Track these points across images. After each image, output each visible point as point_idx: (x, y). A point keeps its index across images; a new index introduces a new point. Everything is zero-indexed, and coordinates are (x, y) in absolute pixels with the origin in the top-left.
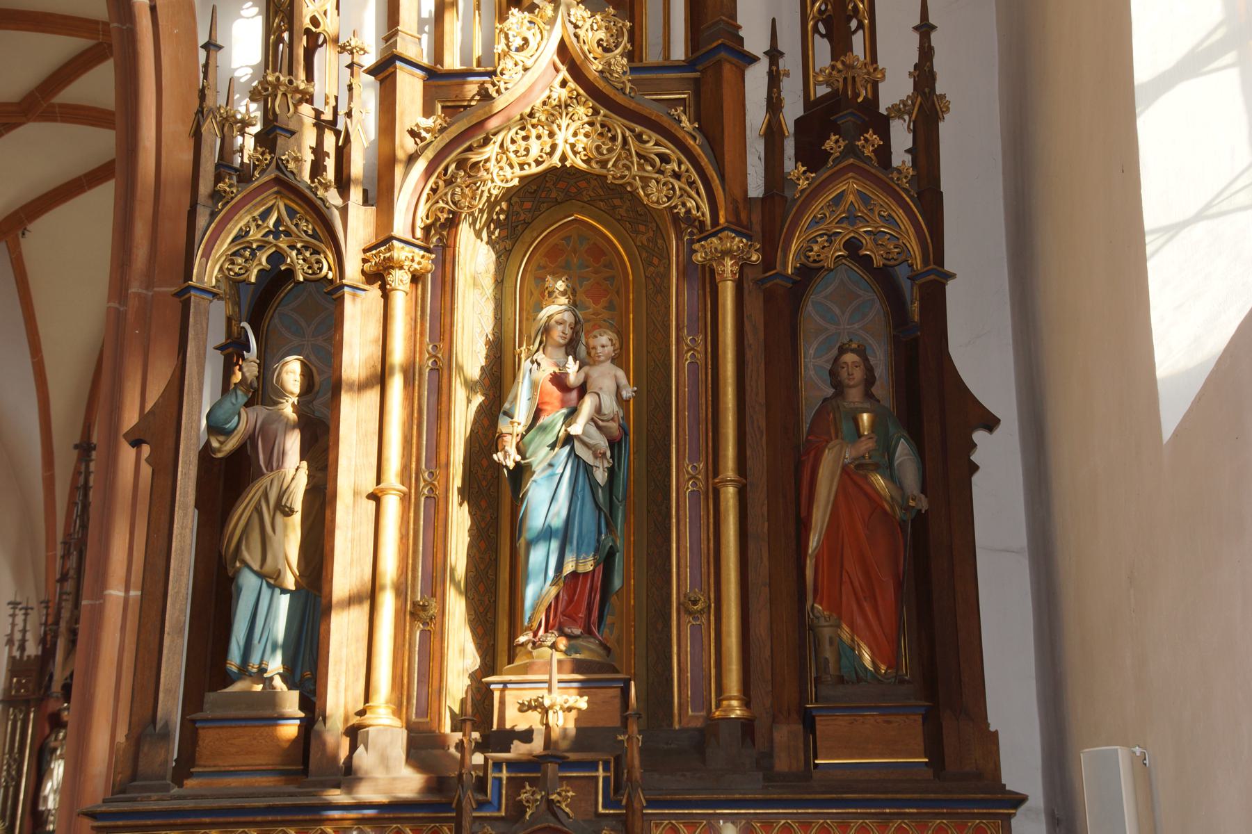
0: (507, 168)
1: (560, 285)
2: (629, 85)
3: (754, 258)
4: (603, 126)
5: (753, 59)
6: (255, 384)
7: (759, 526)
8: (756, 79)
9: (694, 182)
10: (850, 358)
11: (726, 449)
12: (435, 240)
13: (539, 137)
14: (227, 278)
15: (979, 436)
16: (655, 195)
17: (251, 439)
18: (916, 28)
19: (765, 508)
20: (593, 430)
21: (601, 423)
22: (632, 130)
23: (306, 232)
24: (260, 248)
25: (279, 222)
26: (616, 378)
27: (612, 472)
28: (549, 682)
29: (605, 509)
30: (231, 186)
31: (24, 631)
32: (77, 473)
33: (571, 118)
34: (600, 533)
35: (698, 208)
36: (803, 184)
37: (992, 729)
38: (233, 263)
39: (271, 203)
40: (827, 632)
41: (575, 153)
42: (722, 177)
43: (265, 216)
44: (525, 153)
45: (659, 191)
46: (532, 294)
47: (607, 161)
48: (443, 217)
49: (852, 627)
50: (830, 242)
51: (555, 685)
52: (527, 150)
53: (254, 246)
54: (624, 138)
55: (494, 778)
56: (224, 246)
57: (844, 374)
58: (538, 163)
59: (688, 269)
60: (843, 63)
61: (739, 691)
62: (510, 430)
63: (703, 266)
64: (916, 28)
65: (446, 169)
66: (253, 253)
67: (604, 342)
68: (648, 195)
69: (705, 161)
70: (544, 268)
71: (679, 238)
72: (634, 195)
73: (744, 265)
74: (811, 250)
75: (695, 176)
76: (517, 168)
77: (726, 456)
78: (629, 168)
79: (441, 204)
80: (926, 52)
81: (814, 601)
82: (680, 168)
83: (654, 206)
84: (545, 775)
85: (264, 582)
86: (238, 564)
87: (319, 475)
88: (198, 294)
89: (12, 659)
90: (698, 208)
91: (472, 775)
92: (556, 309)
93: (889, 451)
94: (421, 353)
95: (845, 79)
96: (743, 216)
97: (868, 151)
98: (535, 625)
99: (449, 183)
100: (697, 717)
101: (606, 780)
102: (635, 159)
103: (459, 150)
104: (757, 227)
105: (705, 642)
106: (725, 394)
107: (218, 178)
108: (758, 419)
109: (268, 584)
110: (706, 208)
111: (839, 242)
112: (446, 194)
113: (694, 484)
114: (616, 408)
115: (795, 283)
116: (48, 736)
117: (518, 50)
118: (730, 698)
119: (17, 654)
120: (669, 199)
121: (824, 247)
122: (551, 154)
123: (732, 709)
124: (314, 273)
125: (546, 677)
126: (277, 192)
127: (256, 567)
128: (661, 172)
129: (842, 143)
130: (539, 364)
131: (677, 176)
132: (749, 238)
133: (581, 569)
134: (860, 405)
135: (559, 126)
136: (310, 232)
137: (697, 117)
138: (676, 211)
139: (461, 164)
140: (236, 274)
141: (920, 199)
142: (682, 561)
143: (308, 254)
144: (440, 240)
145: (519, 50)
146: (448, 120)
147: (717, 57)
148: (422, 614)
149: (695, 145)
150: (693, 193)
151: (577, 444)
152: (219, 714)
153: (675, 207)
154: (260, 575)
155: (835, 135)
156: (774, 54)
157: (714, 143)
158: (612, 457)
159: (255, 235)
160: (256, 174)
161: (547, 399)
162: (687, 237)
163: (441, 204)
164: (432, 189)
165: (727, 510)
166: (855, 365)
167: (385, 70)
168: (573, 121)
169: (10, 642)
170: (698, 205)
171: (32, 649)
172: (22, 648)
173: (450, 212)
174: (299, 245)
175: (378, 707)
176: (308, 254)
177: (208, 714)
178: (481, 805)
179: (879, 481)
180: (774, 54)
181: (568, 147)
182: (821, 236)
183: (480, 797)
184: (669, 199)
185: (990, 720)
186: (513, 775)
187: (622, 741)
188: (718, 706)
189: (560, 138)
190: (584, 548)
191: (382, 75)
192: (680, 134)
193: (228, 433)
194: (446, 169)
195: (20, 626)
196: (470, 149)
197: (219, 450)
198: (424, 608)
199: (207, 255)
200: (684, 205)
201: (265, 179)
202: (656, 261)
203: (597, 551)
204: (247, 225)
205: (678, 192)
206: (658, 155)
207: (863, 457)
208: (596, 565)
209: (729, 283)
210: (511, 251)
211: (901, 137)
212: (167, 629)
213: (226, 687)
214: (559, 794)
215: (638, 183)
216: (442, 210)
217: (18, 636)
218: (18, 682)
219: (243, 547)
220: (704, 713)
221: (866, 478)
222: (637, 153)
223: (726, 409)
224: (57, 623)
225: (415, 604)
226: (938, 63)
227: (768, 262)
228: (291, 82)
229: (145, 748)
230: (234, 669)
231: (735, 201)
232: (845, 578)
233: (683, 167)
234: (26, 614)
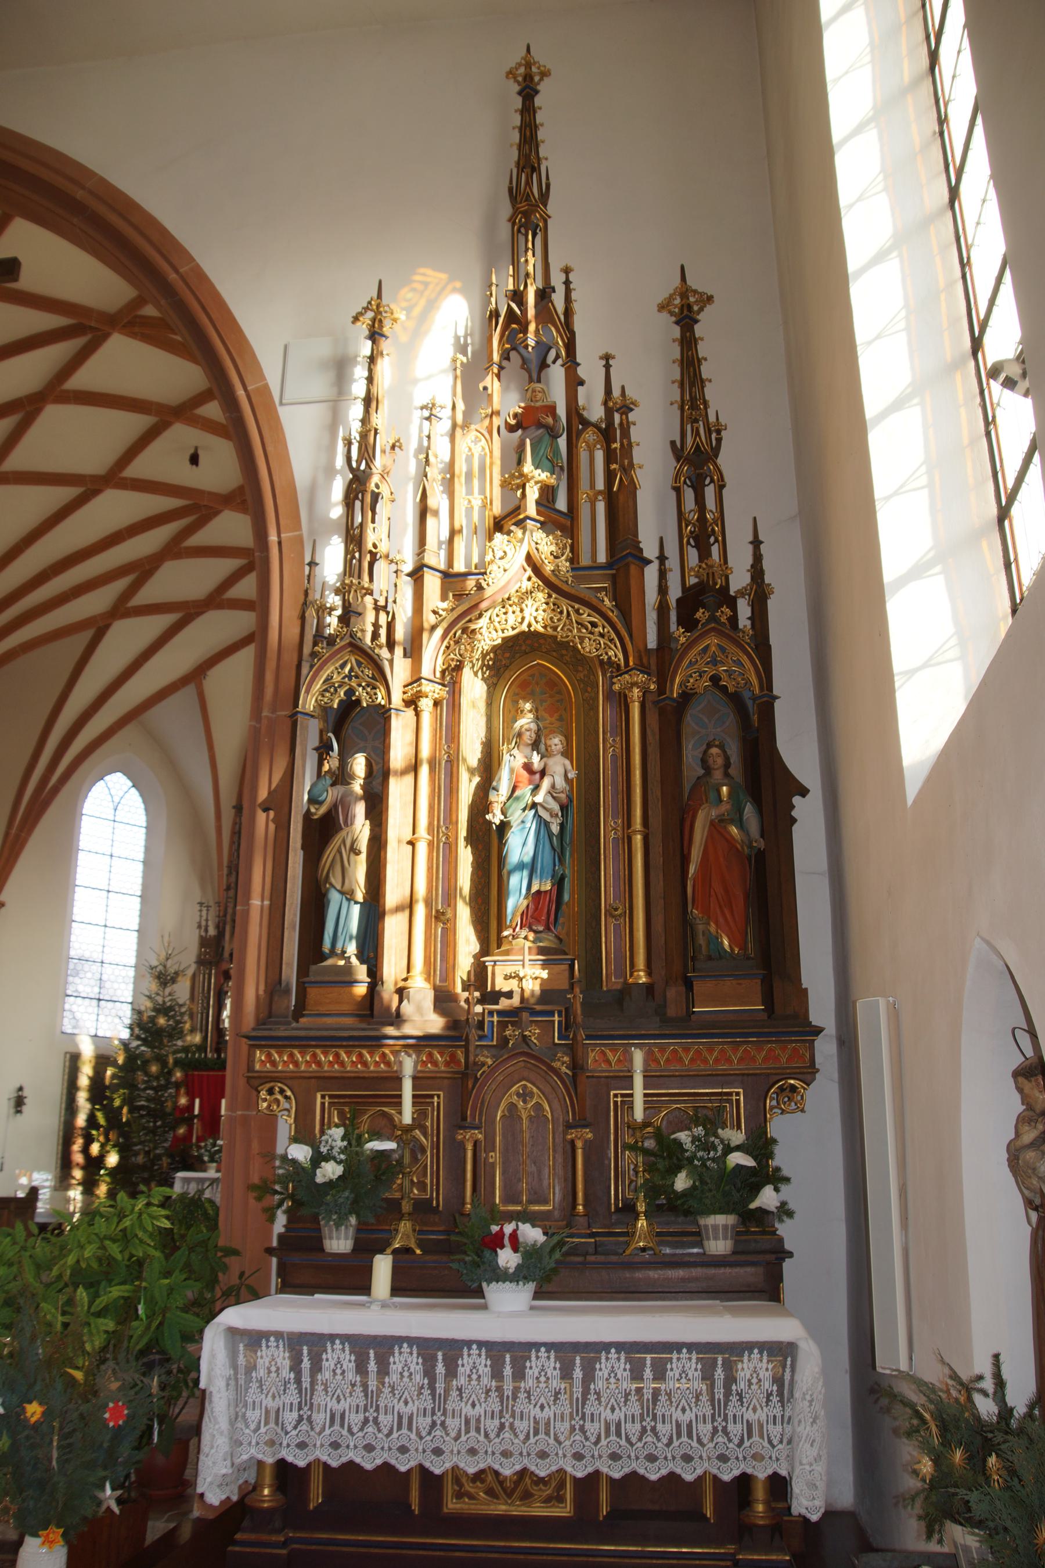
0: (494, 632)
1: (528, 706)
2: (570, 579)
3: (652, 687)
4: (554, 604)
5: (649, 562)
6: (337, 772)
7: (657, 859)
8: (651, 574)
9: (613, 639)
10: (714, 751)
11: (635, 811)
12: (448, 678)
13: (514, 612)
14: (320, 705)
15: (796, 800)
16: (588, 648)
17: (335, 806)
18: (751, 543)
19: (661, 848)
20: (550, 799)
21: (555, 795)
22: (573, 607)
24: (340, 686)
25: (351, 670)
26: (564, 765)
27: (562, 826)
28: (523, 961)
29: (558, 850)
30: (322, 648)
31: (207, 920)
32: (235, 824)
34: (555, 865)
35: (616, 656)
36: (682, 640)
37: (804, 987)
38: (323, 696)
39: (346, 658)
41: (537, 622)
42: (631, 636)
43: (343, 666)
45: (591, 645)
46: (510, 711)
47: (557, 627)
48: (453, 664)
49: (717, 923)
50: (700, 676)
51: (527, 962)
53: (336, 685)
54: (568, 614)
56: (318, 685)
57: (711, 761)
58: (513, 629)
59: (609, 695)
60: (706, 564)
61: (644, 966)
62: (496, 800)
63: (620, 693)
64: (751, 543)
65: (455, 634)
66: (336, 690)
67: (556, 742)
68: (583, 648)
69: (619, 626)
70: (518, 694)
71: (604, 675)
72: (575, 648)
73: (646, 692)
75: (613, 635)
76: (500, 632)
77: (635, 815)
78: (571, 631)
80: (758, 558)
81: (693, 908)
83: (588, 655)
84: (521, 1019)
86: (328, 886)
87: (377, 829)
89: (201, 937)
90: (616, 656)
92: (525, 722)
93: (740, 811)
94: (440, 751)
95: (708, 574)
96: (645, 661)
97: (723, 619)
98: (514, 924)
99: (457, 642)
100: (617, 983)
101: (560, 1022)
102: (575, 625)
103: (463, 622)
104: (654, 667)
105: (623, 933)
107: (315, 644)
108: (656, 791)
109: (347, 898)
110: (621, 656)
111: (706, 677)
112: (455, 650)
113: (615, 833)
114: (564, 784)
115: (678, 702)
116: (223, 984)
118: (639, 971)
119: (203, 934)
120: (597, 650)
122: (521, 623)
123: (639, 977)
124: (373, 701)
125: (521, 958)
126: (351, 651)
127: (339, 887)
128: (592, 633)
129: (707, 614)
131: (602, 635)
132: (649, 674)
133: (543, 889)
134: (719, 781)
135: (527, 606)
136: (370, 676)
137: (614, 598)
139: (464, 630)
140: (326, 703)
141: (756, 649)
142: (608, 883)
143: (369, 689)
144: (452, 678)
145: (501, 558)
146: (456, 603)
147: (627, 561)
148: (442, 918)
149: (613, 616)
150: (613, 646)
151: (539, 808)
152: (319, 979)
153: (601, 655)
154: (342, 893)
156: (662, 558)
158: (562, 816)
159: (337, 678)
160: (338, 640)
161: (520, 780)
162: (609, 675)
163: (452, 656)
165: (636, 850)
166: (718, 755)
167: (417, 574)
169: (199, 927)
170: (615, 654)
171: (212, 931)
172: (206, 931)
173: (457, 661)
174: (363, 684)
176: (369, 689)
177: (312, 978)
178: (481, 1038)
179: (734, 830)
180: (662, 558)
182: (695, 673)
183: (480, 1033)
184: (597, 650)
185: (803, 981)
187: (570, 998)
188: (631, 975)
189: (526, 613)
190: (545, 875)
191: (415, 577)
192: (604, 609)
193: (321, 803)
194: (455, 634)
195: (204, 918)
196: (470, 621)
197: (315, 814)
198: (443, 914)
199: (308, 691)
200: (607, 654)
201: (343, 643)
202: (589, 689)
203: (553, 877)
204: (332, 672)
205: (603, 646)
206: (590, 622)
207: (724, 815)
208: (553, 885)
209: (637, 704)
211: (744, 611)
212: (286, 926)
213: (322, 962)
214: (530, 1031)
215: (577, 640)
216: (453, 660)
217: (203, 923)
218: (205, 951)
219: (331, 875)
220: (621, 980)
221: (725, 828)
222: (577, 622)
223: (635, 784)
224: (225, 915)
225: (437, 911)
226: (766, 564)
227: (661, 690)
228: (359, 583)
229: (276, 998)
230: (327, 951)
231: (639, 651)
232: (712, 893)
234: (208, 910)
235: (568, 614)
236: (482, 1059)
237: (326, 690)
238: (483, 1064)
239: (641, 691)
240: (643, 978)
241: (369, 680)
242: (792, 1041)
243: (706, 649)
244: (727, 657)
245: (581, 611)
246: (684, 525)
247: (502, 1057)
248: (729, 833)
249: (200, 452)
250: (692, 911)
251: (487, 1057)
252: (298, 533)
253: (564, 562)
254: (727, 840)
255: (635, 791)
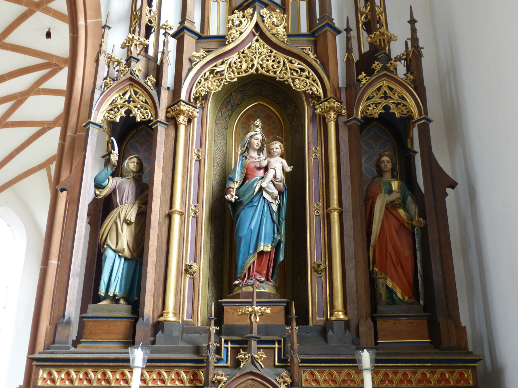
0: (232, 74)
3: (344, 111)
4: (274, 57)
5: (339, 32)
6: (116, 164)
8: (340, 40)
11: (333, 195)
13: (246, 61)
14: (105, 119)
16: (299, 85)
17: (114, 191)
19: (352, 222)
20: (271, 185)
22: (288, 59)
23: (142, 101)
24: (121, 107)
25: (130, 97)
26: (282, 163)
27: (279, 206)
29: (277, 222)
30: (110, 81)
33: (260, 54)
34: (274, 233)
35: (317, 91)
39: (127, 89)
40: (381, 281)
41: (262, 68)
42: (328, 77)
44: (240, 67)
45: (300, 84)
46: (240, 134)
49: (392, 279)
52: (241, 66)
53: (119, 106)
54: (284, 64)
55: (225, 348)
57: (383, 165)
58: (246, 72)
61: (342, 307)
62: (232, 186)
64: (409, 22)
65: (205, 74)
66: (118, 110)
68: (295, 85)
70: (245, 123)
71: (308, 105)
72: (289, 85)
73: (339, 114)
74: (368, 110)
75: (316, 77)
76: (236, 74)
77: (333, 198)
78: (286, 74)
79: (202, 88)
80: (414, 31)
82: (309, 74)
83: (298, 90)
85: (117, 255)
86: (105, 246)
87: (144, 206)
88: (93, 126)
90: (317, 91)
91: (214, 345)
93: (404, 200)
95: (380, 40)
96: (338, 94)
98: (243, 275)
100: (321, 320)
101: (279, 349)
102: (289, 70)
104: (343, 99)
105: (324, 286)
106: (332, 171)
108: (347, 182)
109: (119, 256)
111: (380, 107)
113: (318, 212)
115: (361, 123)
117: (237, 26)
118: (338, 311)
121: (374, 109)
122: (252, 68)
124: (145, 118)
125: (251, 300)
126: (131, 84)
127: (114, 247)
129: (381, 65)
130: (246, 157)
131: (307, 78)
132: (341, 103)
133: (265, 250)
134: (391, 180)
135: (255, 57)
136: (144, 101)
138: (307, 92)
140: (111, 118)
143: (142, 110)
147: (325, 29)
148: (190, 270)
149: (317, 66)
150: (315, 85)
152: (94, 314)
153: (308, 90)
154: (115, 251)
155: (377, 61)
157: (324, 65)
158: (280, 199)
159: (120, 102)
162: (311, 105)
163: (202, 88)
164: (198, 82)
166: (388, 162)
167: (179, 35)
168: (262, 55)
173: (206, 91)
174: (139, 106)
175: (168, 313)
177: (89, 314)
178: (219, 360)
179: (402, 212)
180: (348, 30)
181: (259, 66)
182: (373, 104)
183: (218, 356)
184: (305, 87)
185: (462, 321)
186: (234, 346)
187: (288, 330)
188: (331, 314)
189: (255, 62)
190: (267, 240)
191: (178, 36)
192: (309, 60)
193: (103, 188)
194: (205, 74)
196: (216, 66)
197: (99, 195)
198: (191, 267)
199: (98, 110)
200: (311, 89)
201: (125, 78)
202: (295, 120)
203: (273, 242)
204: (117, 98)
205: (308, 84)
207: (394, 201)
208: (272, 249)
209: (333, 122)
210: (231, 116)
212: (71, 274)
213: (99, 303)
214: (258, 355)
215: (290, 80)
219: (108, 239)
220: (324, 319)
223: (333, 177)
226: (419, 35)
227: (350, 114)
228: (139, 39)
229: (59, 329)
230: (103, 295)
231: (334, 88)
232: (388, 256)
233: (310, 74)
235: (284, 64)
236: (219, 378)
237: (111, 110)
238: (220, 382)
239: (335, 114)
240: (341, 316)
241: (143, 103)
242: (458, 367)
243: (379, 89)
244: (394, 94)
245: (293, 61)
246: (359, 15)
247: (235, 375)
248: (399, 213)
249: (51, 31)
250: (373, 269)
251: (222, 376)
252: (99, 20)
253: (282, 29)
254: (397, 219)
255: (333, 182)
